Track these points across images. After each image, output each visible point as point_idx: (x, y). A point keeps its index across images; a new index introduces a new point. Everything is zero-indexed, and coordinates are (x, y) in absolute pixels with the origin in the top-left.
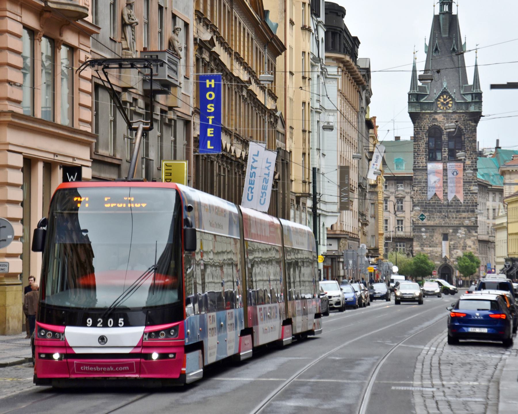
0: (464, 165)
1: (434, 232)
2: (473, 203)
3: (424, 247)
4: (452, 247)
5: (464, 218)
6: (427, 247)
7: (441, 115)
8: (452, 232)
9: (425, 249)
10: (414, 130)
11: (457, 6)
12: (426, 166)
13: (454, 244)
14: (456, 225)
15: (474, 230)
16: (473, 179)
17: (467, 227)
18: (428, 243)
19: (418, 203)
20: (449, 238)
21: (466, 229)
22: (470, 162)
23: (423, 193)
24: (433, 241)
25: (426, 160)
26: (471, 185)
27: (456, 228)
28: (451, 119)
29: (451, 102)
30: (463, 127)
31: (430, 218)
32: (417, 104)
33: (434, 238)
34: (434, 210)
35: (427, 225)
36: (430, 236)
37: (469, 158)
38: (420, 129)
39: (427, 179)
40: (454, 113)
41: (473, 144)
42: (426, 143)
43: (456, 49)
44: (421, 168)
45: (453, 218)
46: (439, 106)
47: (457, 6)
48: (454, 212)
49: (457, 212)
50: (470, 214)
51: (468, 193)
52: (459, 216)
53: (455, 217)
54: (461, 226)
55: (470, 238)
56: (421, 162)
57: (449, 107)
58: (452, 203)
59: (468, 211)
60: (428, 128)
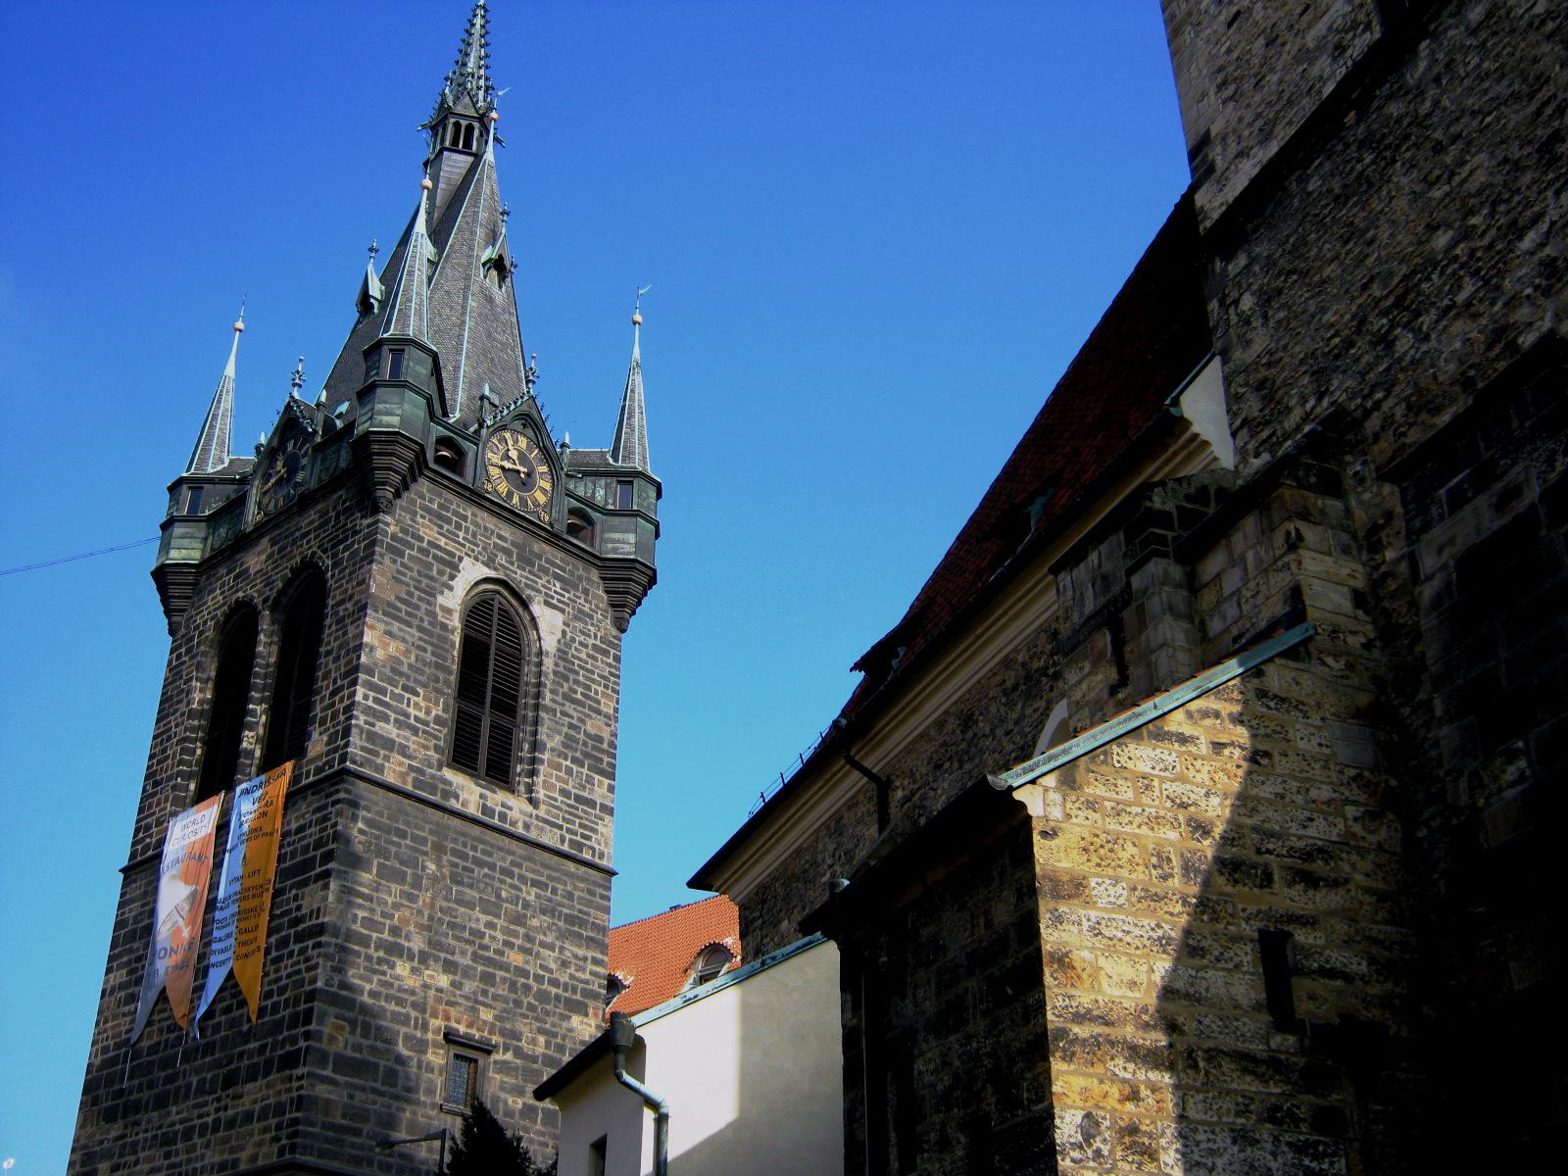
5: (248, 1117)
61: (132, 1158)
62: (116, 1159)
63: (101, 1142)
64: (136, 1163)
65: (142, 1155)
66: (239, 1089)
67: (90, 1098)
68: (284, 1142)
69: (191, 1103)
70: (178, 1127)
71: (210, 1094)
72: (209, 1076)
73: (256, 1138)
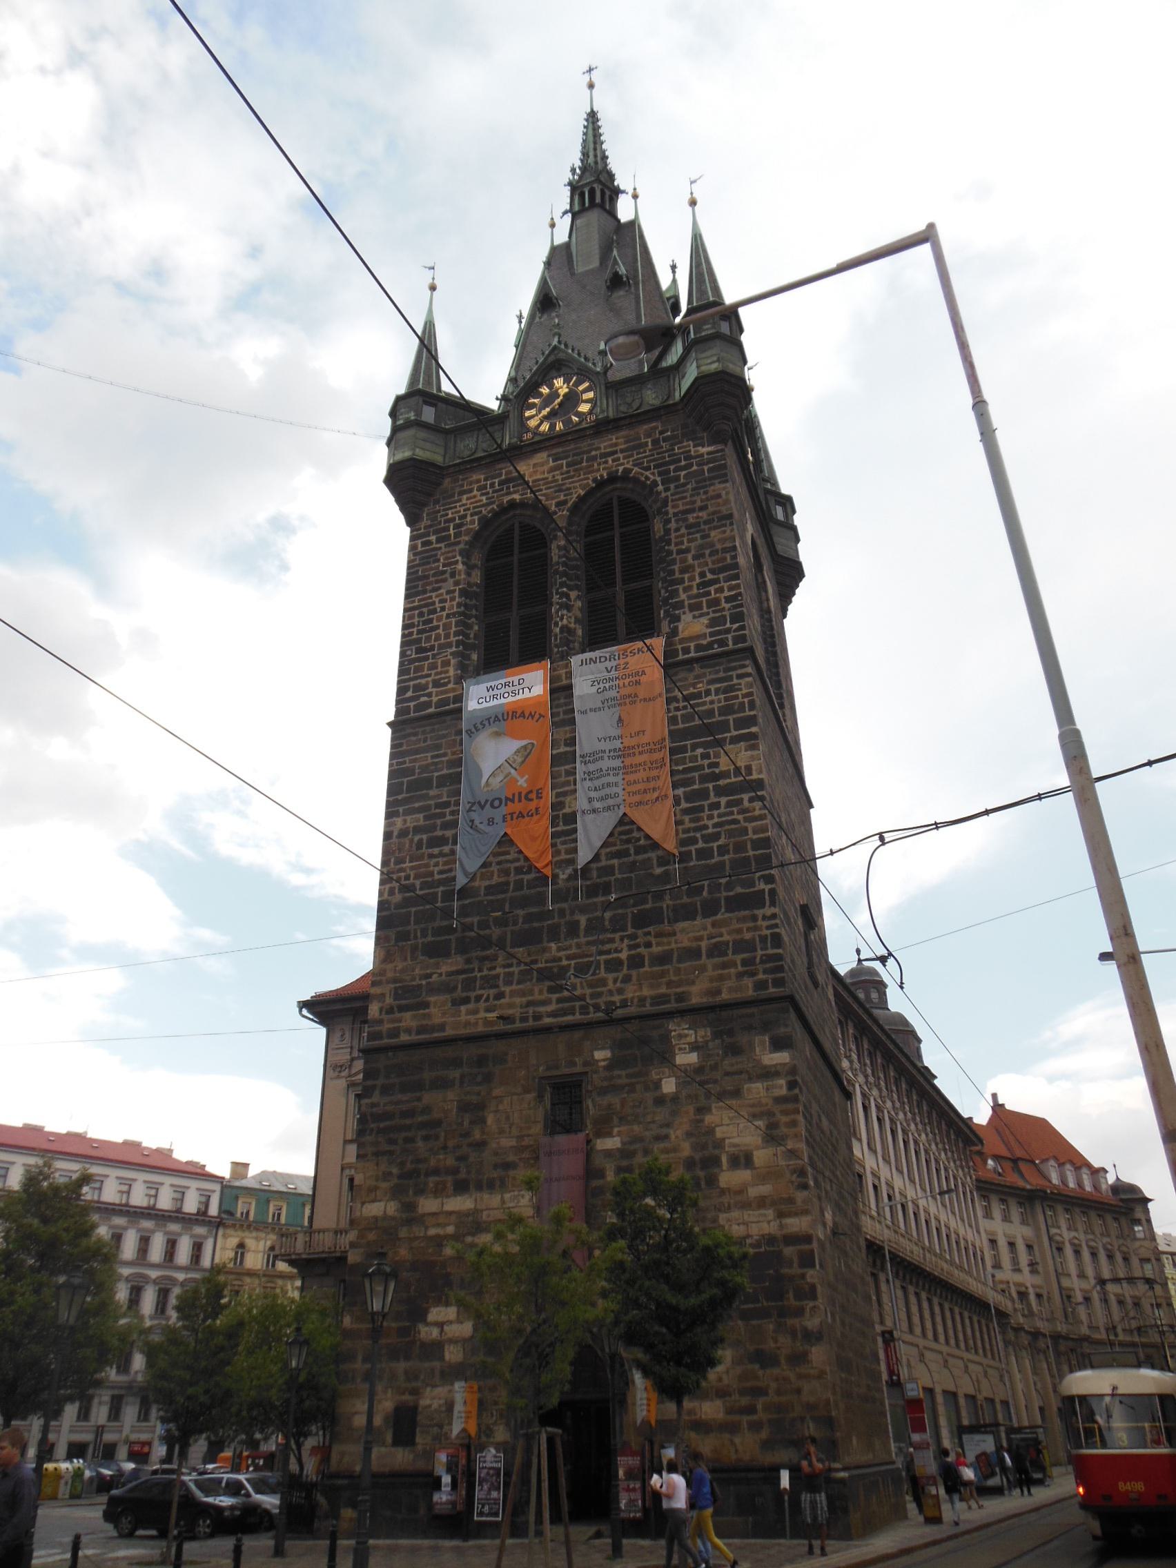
0: (669, 644)
1: (488, 1078)
2: (740, 847)
3: (421, 1191)
4: (611, 1177)
5: (694, 953)
6: (439, 1192)
7: (541, 457)
8: (613, 1064)
9: (428, 1205)
10: (412, 548)
11: (635, 197)
12: (459, 699)
13: (625, 1153)
14: (632, 1010)
15: (766, 1027)
16: (726, 710)
17: (714, 1013)
18: (450, 1161)
19: (406, 903)
20: (592, 1107)
21: (704, 1033)
22: (705, 620)
23: (434, 842)
24: (481, 1145)
25: (462, 667)
26: (720, 743)
27: (642, 1039)
28: (594, 458)
29: (591, 395)
30: (652, 476)
31: (469, 984)
32: (422, 434)
33: (490, 1119)
34: (496, 932)
35: (449, 1032)
36: (464, 1107)
37: (692, 608)
38: (438, 541)
39: (459, 763)
40: (603, 427)
41: (713, 534)
42: (463, 593)
43: (622, 270)
44: (432, 710)
45: (613, 966)
46: (532, 423)
47: (635, 197)
48: (618, 925)
49: (642, 920)
50: (730, 925)
51: (704, 794)
52: (656, 949)
53: (624, 955)
54: (670, 1015)
55: (737, 1093)
56: (436, 684)
57: (578, 414)
58: (609, 870)
59: (710, 909)
60: (476, 526)
61: (492, 992)
62: (459, 993)
63: (429, 976)
64: (500, 996)
65: (507, 989)
66: (666, 927)
67: (392, 934)
68: (761, 976)
69: (583, 940)
70: (565, 963)
71: (614, 931)
72: (608, 915)
73: (710, 972)
